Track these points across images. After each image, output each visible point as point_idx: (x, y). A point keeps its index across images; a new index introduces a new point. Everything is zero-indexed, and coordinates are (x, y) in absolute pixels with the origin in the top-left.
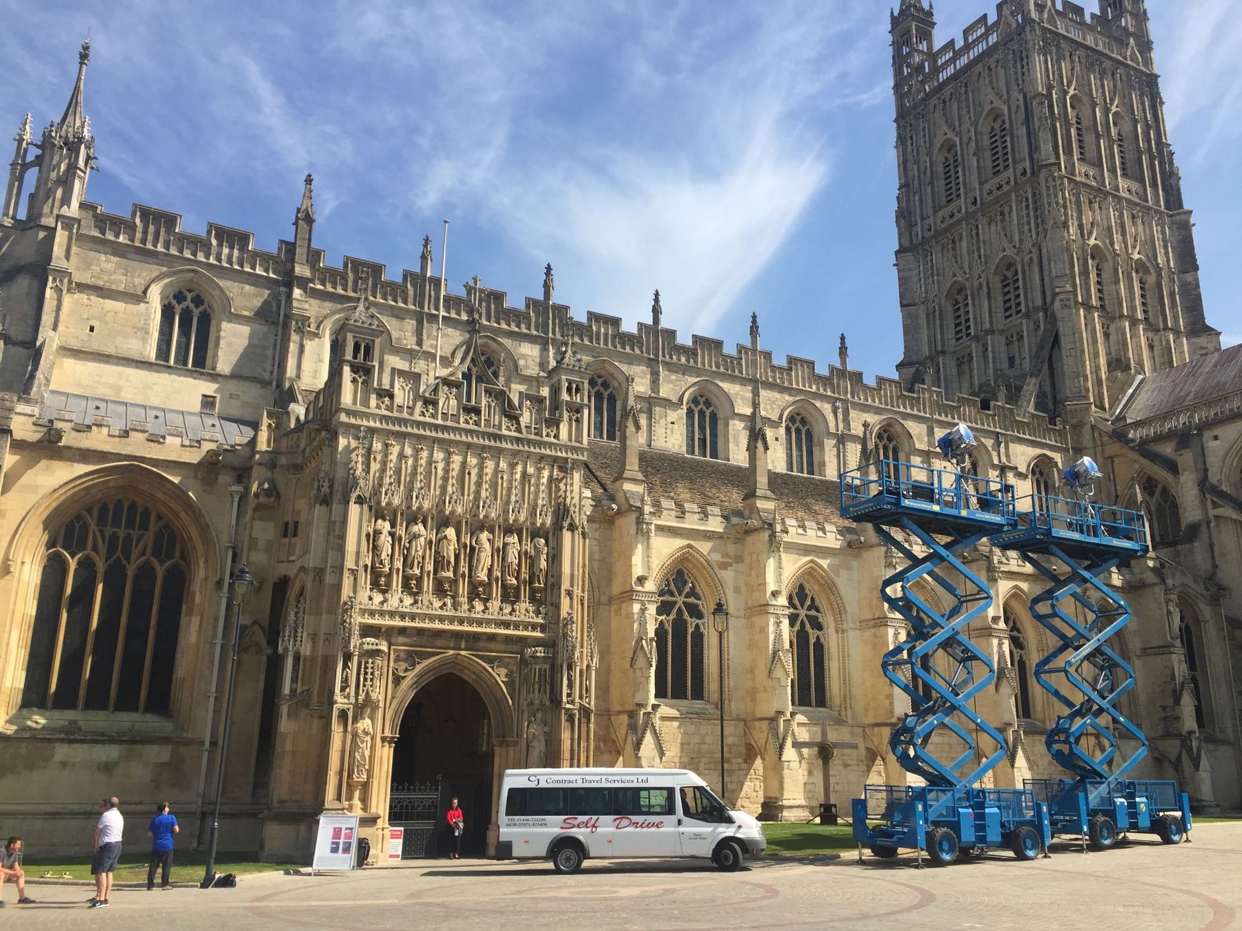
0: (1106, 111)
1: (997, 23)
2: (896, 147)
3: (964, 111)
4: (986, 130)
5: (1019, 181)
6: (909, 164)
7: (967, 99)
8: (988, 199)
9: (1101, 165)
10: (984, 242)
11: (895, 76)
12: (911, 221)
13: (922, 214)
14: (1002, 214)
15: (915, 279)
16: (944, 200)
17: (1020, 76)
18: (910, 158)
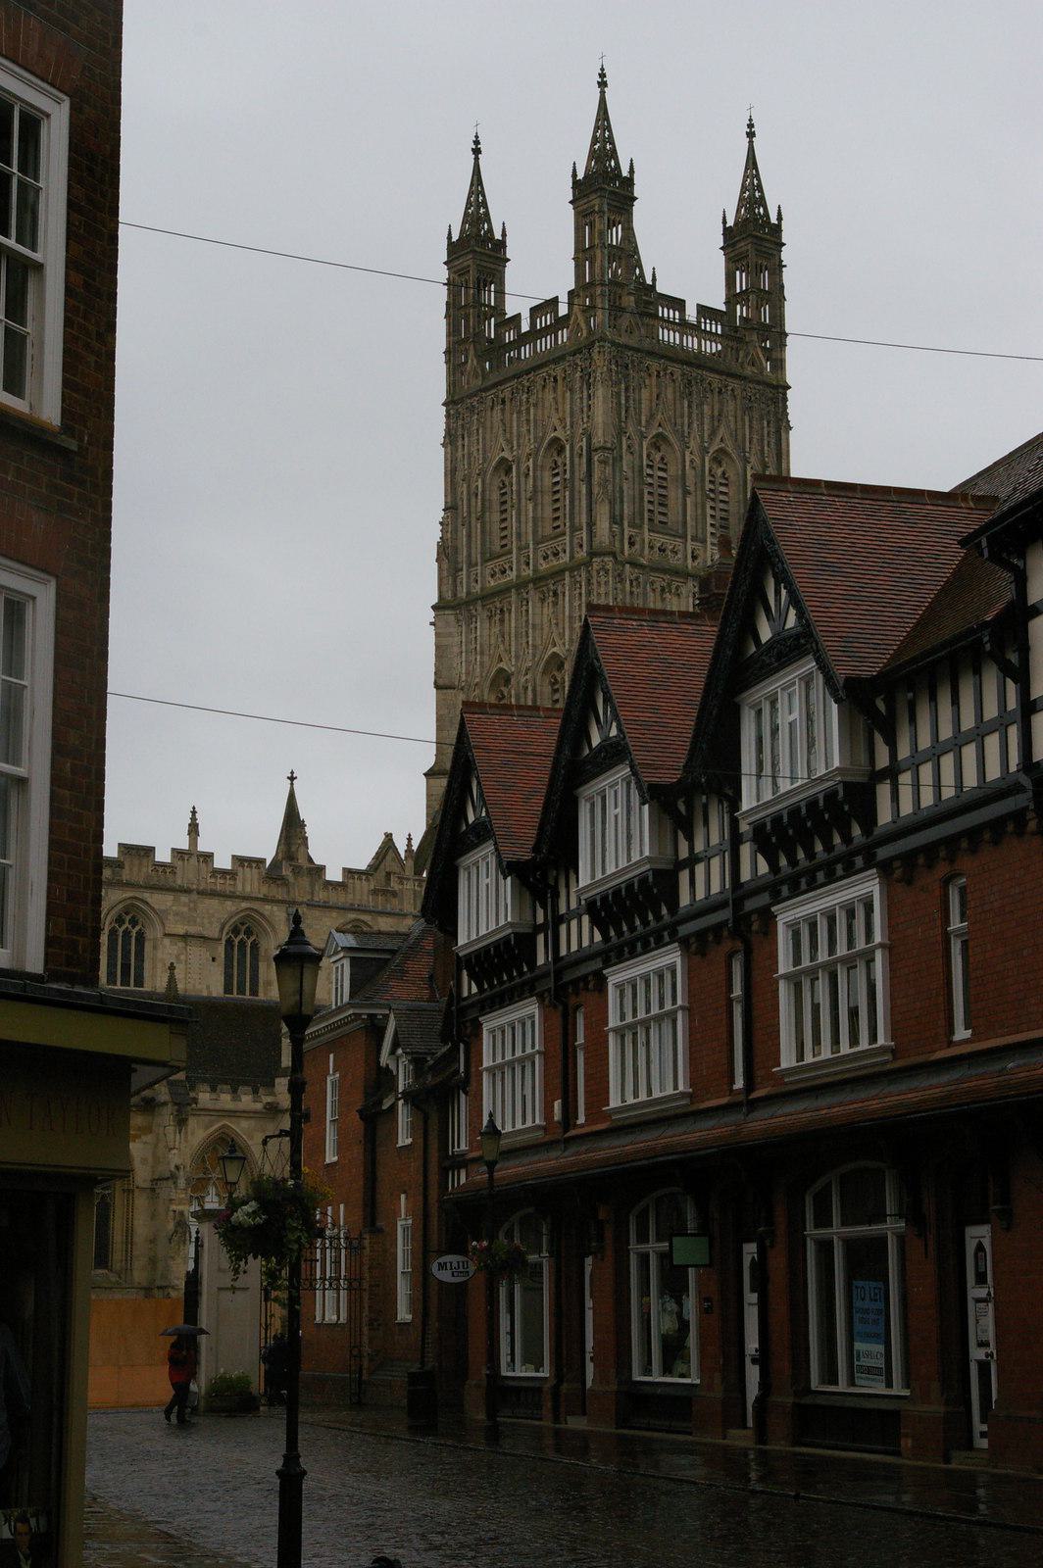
0: (704, 450)
1: (567, 317)
2: (443, 445)
3: (524, 429)
4: (549, 463)
5: (576, 556)
6: (459, 475)
7: (528, 409)
8: (544, 566)
9: (684, 537)
10: (534, 626)
11: (449, 335)
12: (457, 562)
13: (469, 555)
14: (555, 594)
15: (456, 650)
16: (497, 548)
17: (585, 409)
18: (460, 466)
